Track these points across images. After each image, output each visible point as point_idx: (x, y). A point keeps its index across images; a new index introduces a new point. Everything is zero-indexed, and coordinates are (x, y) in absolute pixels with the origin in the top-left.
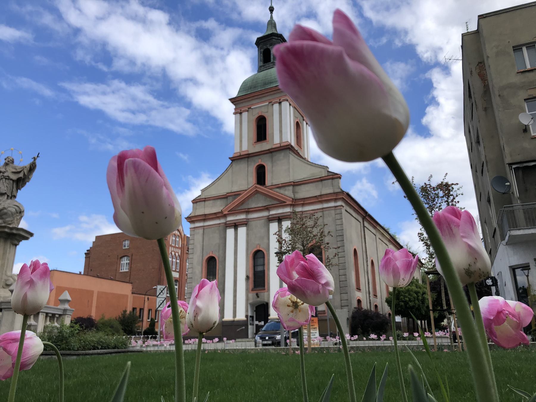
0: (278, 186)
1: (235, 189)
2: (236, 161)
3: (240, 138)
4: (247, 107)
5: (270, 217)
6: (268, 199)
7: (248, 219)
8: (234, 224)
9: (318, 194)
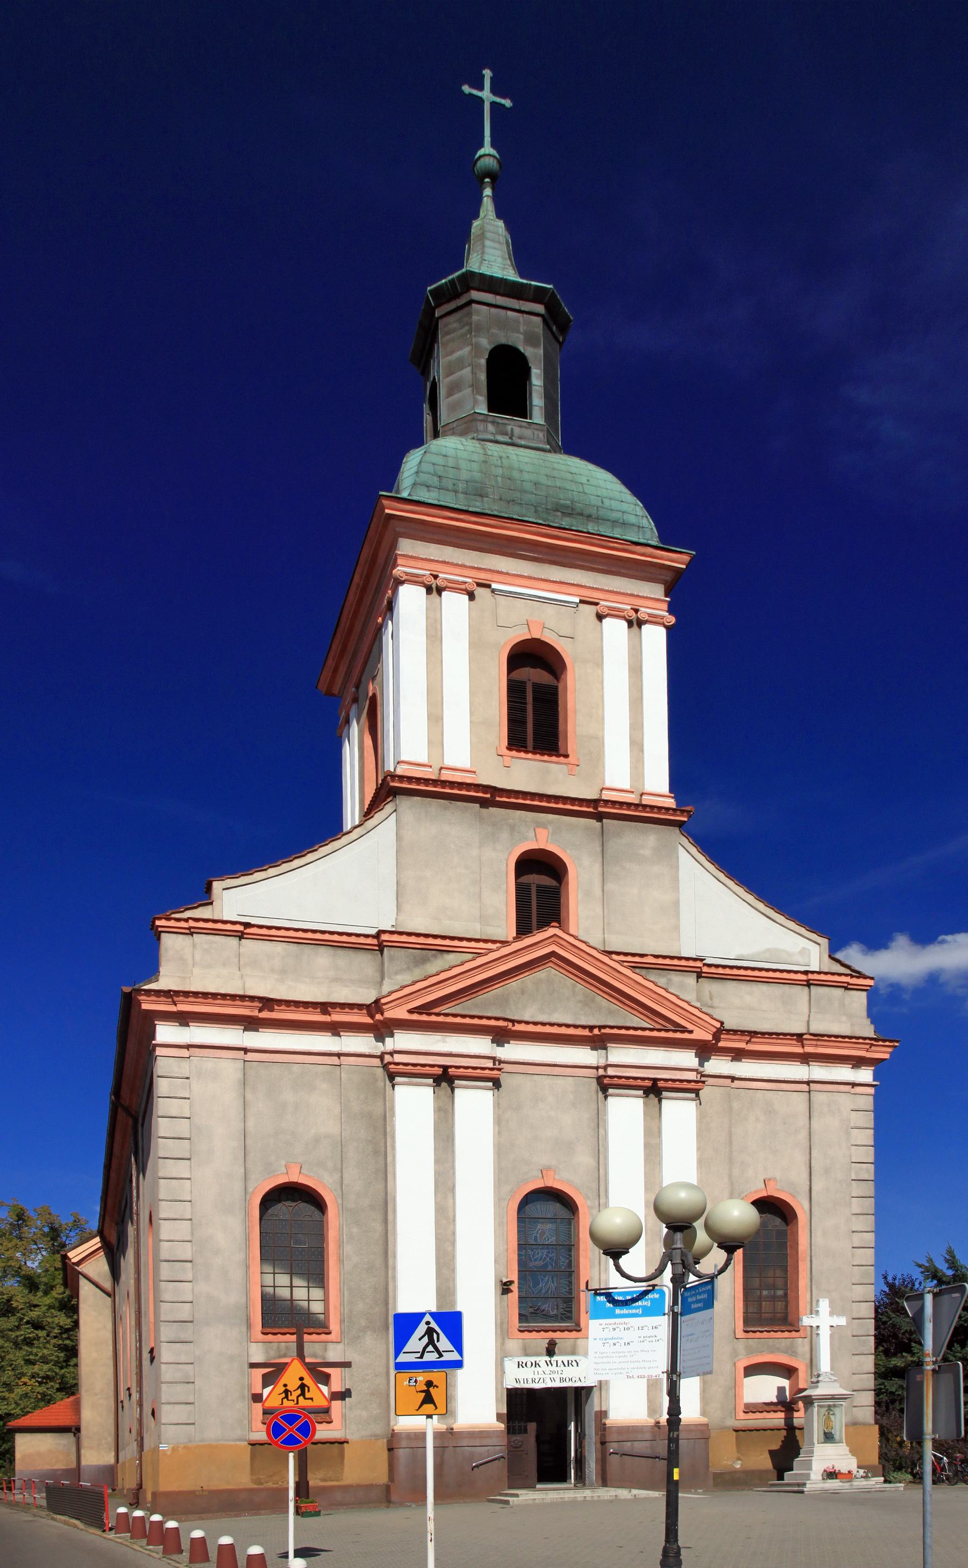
0: (637, 959)
1: (419, 923)
2: (417, 799)
3: (430, 704)
4: (466, 572)
5: (611, 1072)
6: (603, 1002)
7: (500, 1062)
8: (439, 1071)
9: (799, 1028)
